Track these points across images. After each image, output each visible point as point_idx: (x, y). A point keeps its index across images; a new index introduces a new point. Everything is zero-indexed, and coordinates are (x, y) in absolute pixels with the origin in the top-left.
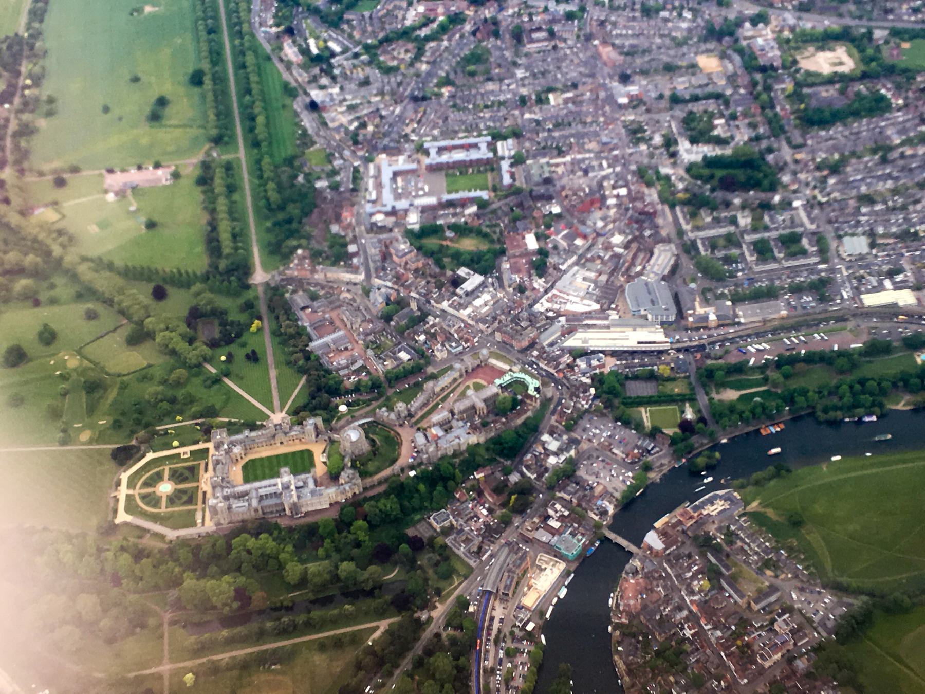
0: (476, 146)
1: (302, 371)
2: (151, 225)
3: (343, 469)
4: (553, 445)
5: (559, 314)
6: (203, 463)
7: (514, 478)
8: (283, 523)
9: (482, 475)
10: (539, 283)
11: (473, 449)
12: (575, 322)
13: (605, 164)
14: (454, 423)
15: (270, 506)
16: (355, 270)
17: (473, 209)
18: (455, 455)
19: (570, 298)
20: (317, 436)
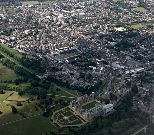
8: (105, 115)
11: (130, 92)
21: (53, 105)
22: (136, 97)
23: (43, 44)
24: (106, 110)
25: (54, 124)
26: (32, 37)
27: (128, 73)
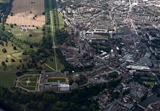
0: (104, 31)
1: (63, 64)
2: (31, 36)
3: (73, 82)
4: (125, 86)
5: (124, 61)
6: (38, 78)
7: (115, 91)
8: (57, 92)
9: (107, 90)
10: (120, 56)
11: (105, 83)
12: (128, 64)
13: (133, 38)
14: (100, 78)
15: (55, 88)
16: (77, 48)
17: (104, 41)
18: (101, 84)
19: (127, 59)
20: (67, 76)
21: (33, 70)
22: (108, 89)
23: (91, 22)
24: (61, 88)
25: (15, 83)
26: (90, 14)
27: (130, 67)
